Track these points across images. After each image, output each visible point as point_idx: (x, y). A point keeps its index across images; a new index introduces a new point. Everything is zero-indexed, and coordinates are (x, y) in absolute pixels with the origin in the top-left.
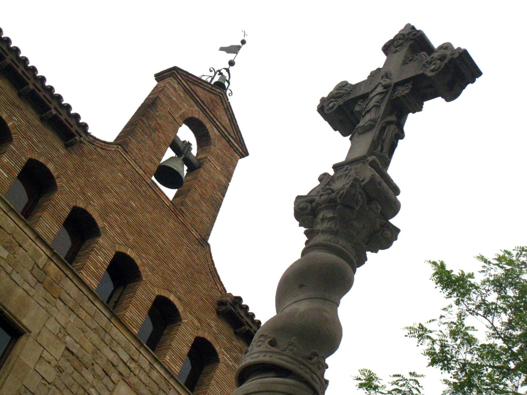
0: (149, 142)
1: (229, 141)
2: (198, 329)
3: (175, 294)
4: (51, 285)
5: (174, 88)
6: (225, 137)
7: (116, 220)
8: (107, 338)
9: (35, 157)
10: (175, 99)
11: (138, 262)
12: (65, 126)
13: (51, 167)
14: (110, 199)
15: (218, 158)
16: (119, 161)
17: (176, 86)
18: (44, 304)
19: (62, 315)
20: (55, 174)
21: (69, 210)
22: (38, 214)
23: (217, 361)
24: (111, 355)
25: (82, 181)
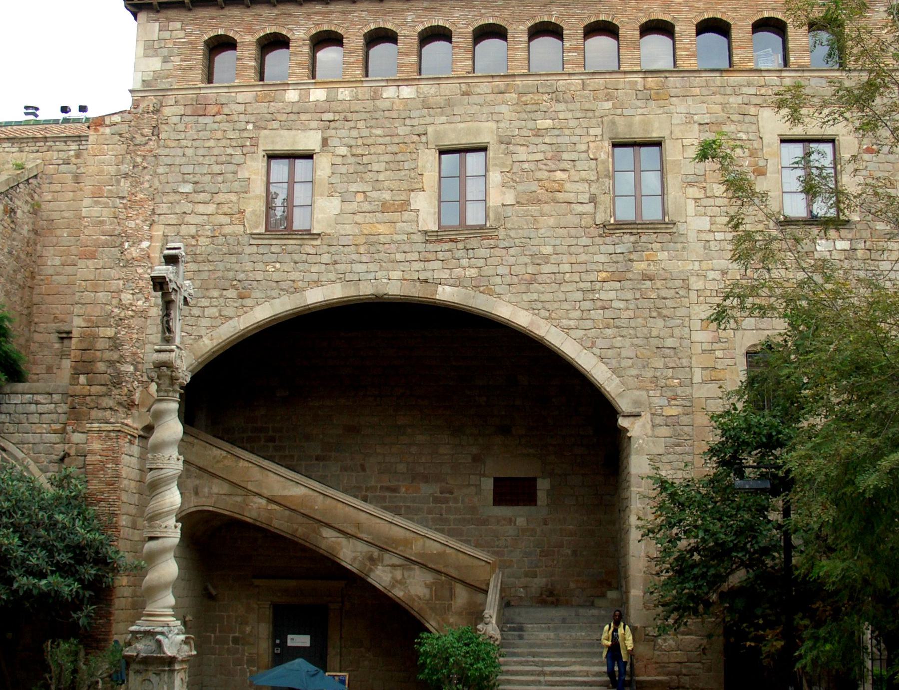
19: (680, 107)
24: (739, 99)
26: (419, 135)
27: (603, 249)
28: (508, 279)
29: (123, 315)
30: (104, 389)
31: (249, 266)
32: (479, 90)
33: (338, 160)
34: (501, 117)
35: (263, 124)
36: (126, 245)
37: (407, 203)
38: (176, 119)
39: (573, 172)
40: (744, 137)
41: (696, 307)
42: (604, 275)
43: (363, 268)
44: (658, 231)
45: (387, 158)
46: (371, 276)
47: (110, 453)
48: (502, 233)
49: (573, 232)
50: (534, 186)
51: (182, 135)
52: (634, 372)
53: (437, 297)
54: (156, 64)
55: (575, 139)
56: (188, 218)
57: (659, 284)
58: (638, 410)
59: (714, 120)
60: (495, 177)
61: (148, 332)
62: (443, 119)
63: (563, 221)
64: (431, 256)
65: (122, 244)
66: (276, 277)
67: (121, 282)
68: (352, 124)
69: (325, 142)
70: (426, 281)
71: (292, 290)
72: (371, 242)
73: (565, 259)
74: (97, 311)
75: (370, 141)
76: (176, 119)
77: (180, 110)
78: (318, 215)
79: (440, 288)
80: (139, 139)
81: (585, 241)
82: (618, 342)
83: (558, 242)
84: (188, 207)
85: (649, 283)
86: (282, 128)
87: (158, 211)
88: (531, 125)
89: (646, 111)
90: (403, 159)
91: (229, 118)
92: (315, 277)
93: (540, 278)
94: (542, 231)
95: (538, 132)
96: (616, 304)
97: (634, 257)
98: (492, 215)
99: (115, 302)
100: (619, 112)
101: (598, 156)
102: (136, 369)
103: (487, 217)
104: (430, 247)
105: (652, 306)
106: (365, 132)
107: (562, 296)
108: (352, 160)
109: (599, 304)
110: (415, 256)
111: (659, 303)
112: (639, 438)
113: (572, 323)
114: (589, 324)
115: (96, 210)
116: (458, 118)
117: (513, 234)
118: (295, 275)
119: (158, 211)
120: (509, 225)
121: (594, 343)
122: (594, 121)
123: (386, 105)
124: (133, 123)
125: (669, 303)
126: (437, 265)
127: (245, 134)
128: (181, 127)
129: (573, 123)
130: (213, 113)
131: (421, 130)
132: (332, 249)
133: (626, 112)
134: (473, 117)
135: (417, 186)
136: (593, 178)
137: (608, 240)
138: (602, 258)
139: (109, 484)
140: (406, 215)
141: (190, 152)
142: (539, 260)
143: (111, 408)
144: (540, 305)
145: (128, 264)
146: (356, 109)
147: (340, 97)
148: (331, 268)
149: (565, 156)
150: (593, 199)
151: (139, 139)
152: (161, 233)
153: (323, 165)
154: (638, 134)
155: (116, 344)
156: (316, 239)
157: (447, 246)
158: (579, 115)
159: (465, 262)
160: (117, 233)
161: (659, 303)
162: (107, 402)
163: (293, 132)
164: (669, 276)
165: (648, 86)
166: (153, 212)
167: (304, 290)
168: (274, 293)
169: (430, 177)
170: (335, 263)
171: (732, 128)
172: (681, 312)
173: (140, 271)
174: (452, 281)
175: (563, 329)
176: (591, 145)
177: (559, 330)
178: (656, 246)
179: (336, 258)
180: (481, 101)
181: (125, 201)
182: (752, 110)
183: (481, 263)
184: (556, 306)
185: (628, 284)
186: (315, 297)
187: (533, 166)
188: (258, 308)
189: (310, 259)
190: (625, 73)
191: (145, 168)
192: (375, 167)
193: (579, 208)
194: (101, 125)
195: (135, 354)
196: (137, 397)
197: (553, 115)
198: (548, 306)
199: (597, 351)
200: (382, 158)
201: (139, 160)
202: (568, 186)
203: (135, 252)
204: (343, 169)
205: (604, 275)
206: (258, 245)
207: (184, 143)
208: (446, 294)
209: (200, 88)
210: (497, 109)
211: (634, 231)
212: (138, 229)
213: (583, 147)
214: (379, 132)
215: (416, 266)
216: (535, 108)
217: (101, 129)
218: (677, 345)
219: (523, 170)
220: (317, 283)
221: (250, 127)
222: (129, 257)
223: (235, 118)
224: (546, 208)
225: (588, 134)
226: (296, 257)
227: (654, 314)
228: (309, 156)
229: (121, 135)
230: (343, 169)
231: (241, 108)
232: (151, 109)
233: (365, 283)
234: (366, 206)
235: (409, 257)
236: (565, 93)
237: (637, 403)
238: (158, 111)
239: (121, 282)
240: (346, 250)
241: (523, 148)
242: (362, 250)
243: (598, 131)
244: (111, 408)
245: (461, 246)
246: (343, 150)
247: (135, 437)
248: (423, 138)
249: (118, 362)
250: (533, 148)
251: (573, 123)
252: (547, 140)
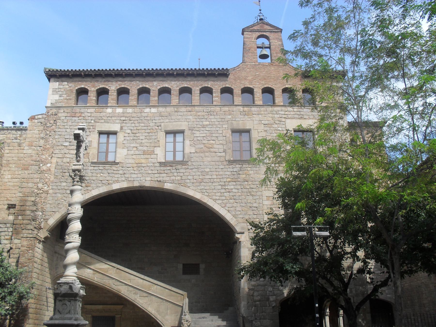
1: (274, 32)
6: (272, 32)
8: (274, 112)
11: (270, 86)
12: (223, 74)
14: (250, 78)
17: (247, 33)
18: (250, 119)
19: (256, 118)
24: (278, 116)
25: (238, 81)
26: (158, 126)
27: (229, 170)
28: (192, 181)
29: (38, 192)
30: (29, 221)
31: (90, 174)
32: (181, 111)
33: (127, 135)
34: (189, 120)
35: (98, 121)
36: (41, 165)
37: (154, 151)
38: (63, 118)
39: (217, 141)
40: (281, 129)
41: (264, 191)
42: (229, 179)
43: (136, 176)
45: (147, 134)
46: (139, 179)
47: (31, 246)
48: (190, 163)
49: (217, 163)
50: (202, 146)
51: (66, 124)
52: (241, 216)
53: (165, 187)
54: (57, 97)
55: (218, 129)
56: (67, 155)
57: (250, 183)
58: (243, 231)
59: (269, 123)
60: (187, 142)
61: (48, 199)
62: (167, 121)
63: (214, 159)
64: (162, 172)
65: (39, 165)
66: (101, 179)
67: (38, 179)
68: (132, 122)
69: (121, 128)
70: (160, 181)
71: (107, 184)
72: (139, 165)
73: (214, 173)
74: (28, 190)
75: (139, 128)
76: (63, 118)
77: (66, 114)
78: (118, 155)
79: (166, 184)
80: (48, 125)
81: (222, 167)
82: (235, 205)
83: (211, 167)
84: (67, 151)
85: (246, 182)
86: (105, 122)
87: (54, 152)
88: (201, 123)
89: (244, 119)
90: (152, 135)
91: (84, 118)
92: (116, 179)
93: (205, 180)
94: (205, 163)
95: (204, 126)
96: (234, 190)
97: (240, 173)
98: (186, 156)
99: (35, 187)
100: (234, 119)
101: (226, 135)
102: (43, 214)
103: (184, 157)
104: (162, 168)
105: (248, 191)
106: (137, 125)
107: (213, 187)
108: (133, 135)
109: (227, 190)
110: (156, 172)
111: (250, 190)
112: (244, 242)
113: (217, 198)
114: (224, 198)
115: (30, 151)
116: (173, 120)
117: (194, 163)
118: (108, 178)
119: (54, 152)
120: (192, 160)
121: (226, 205)
122: (225, 122)
123: (146, 115)
124: (46, 119)
125: (254, 190)
126: (165, 175)
127: (91, 124)
128: (65, 121)
129: (217, 123)
130: (78, 116)
131: (158, 124)
132: (123, 169)
133: (237, 120)
134: (179, 120)
135: (157, 145)
136: (224, 143)
137: (231, 166)
138: (228, 173)
139: (29, 259)
140: (153, 156)
141: (67, 130)
142: (204, 173)
143: (31, 230)
144: (205, 191)
145: (42, 172)
146: (134, 116)
147: (128, 112)
148: (123, 176)
149: (214, 135)
150: (225, 151)
151: (48, 125)
152: (55, 161)
153: (121, 136)
154: (241, 127)
155: (35, 204)
156: (117, 165)
157: (169, 168)
158: (219, 120)
159: (176, 174)
160: (38, 160)
161: (250, 190)
162: (29, 227)
163: (109, 124)
164: (254, 180)
165: (244, 110)
166: (53, 153)
167: (112, 184)
168: (100, 185)
169: (162, 142)
170: (125, 174)
171: (276, 126)
172: (259, 193)
173: (46, 175)
174: (170, 181)
175: (214, 200)
176: (224, 131)
177: (212, 200)
178: (249, 169)
179: (125, 172)
180: (182, 114)
181: (41, 148)
182: (283, 120)
183: (182, 174)
184: (211, 191)
185: (238, 183)
186: (116, 186)
187: (201, 138)
188: (93, 191)
189: (115, 172)
190: (236, 105)
191: (50, 136)
192: (141, 138)
193: (219, 154)
194: (34, 119)
195: (42, 208)
196: (42, 225)
197: (209, 120)
198: (207, 191)
199: (227, 208)
200: (144, 134)
201: (48, 132)
202: (215, 146)
203: (44, 168)
204: (128, 138)
205: (229, 179)
206: (94, 167)
207: (66, 127)
208: (168, 186)
209: (73, 107)
210: (188, 117)
212: (46, 159)
213: (221, 132)
214: (143, 125)
215: (157, 175)
216: (202, 117)
217: (33, 120)
218: (257, 206)
219: (198, 140)
220: (117, 181)
221: (93, 121)
222: (42, 170)
223: (87, 118)
224: (207, 154)
225: (222, 127)
226: (109, 171)
227: (249, 194)
228: (115, 133)
229: (41, 123)
230: (128, 138)
231: (89, 114)
232: (54, 113)
233: (136, 182)
234: (137, 152)
235: (154, 172)
236: (213, 112)
237: (242, 228)
238: (56, 114)
239: (38, 179)
240: (129, 169)
241: (198, 132)
242: (135, 169)
243: (226, 126)
244: (31, 230)
245: (174, 168)
246: (129, 131)
247: (41, 241)
248: (160, 128)
249: (35, 211)
250: (201, 132)
251: (217, 123)
252: (207, 129)
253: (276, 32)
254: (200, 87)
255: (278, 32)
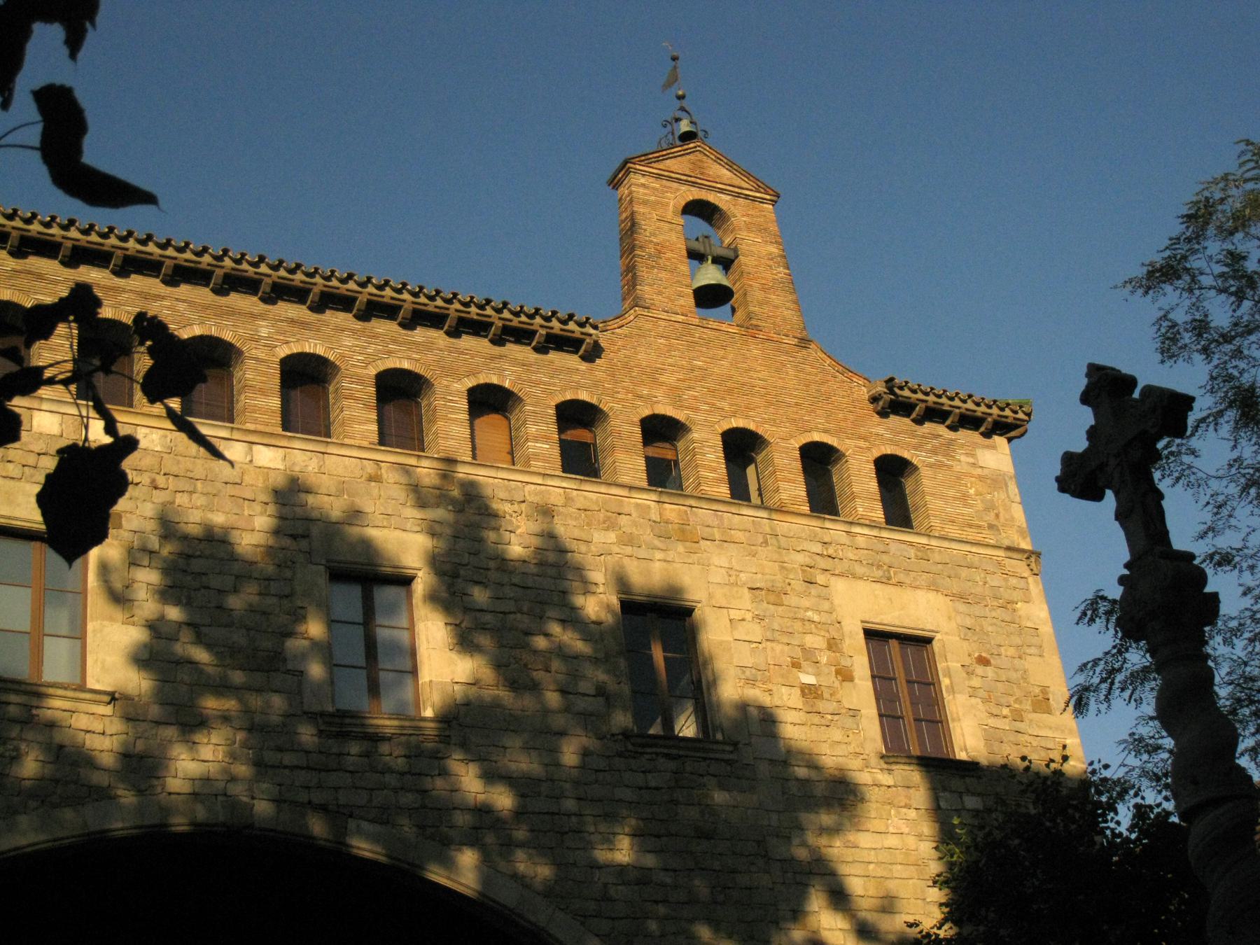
0: (663, 275)
1: (747, 197)
2: (869, 449)
3: (818, 430)
4: (683, 531)
5: (643, 185)
6: (739, 195)
7: (695, 398)
9: (560, 398)
10: (653, 198)
11: (752, 427)
13: (584, 396)
14: (669, 379)
15: (748, 227)
16: (648, 326)
17: (643, 180)
20: (594, 401)
21: (638, 430)
22: (609, 461)
23: (916, 468)
40: (816, 618)
44: (712, 755)
211: (674, 752)
253: (754, 199)
254: (470, 383)
255: (762, 201)
